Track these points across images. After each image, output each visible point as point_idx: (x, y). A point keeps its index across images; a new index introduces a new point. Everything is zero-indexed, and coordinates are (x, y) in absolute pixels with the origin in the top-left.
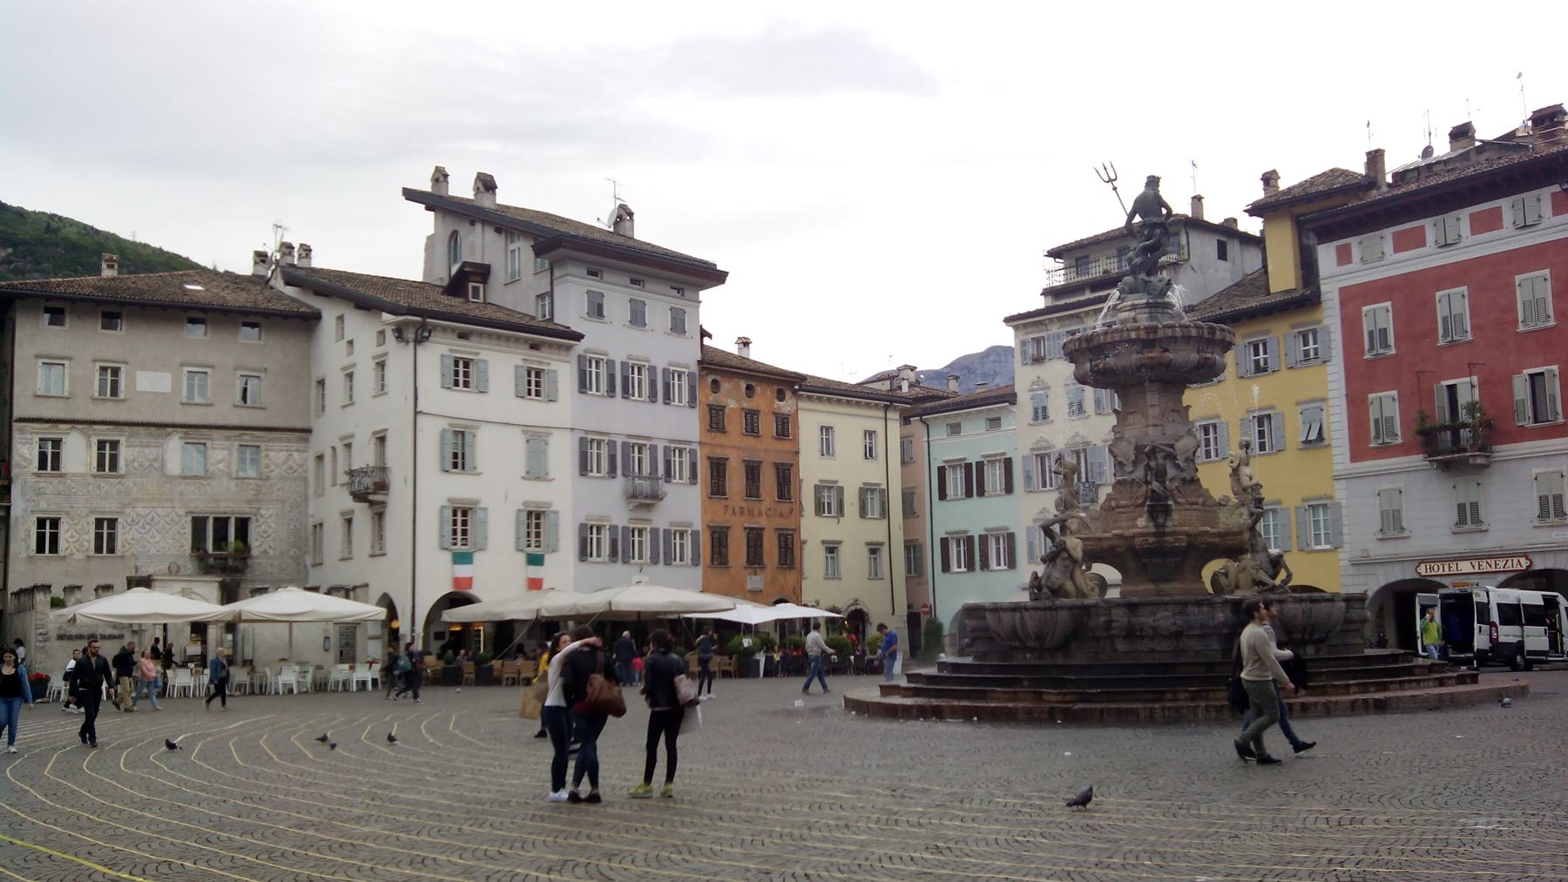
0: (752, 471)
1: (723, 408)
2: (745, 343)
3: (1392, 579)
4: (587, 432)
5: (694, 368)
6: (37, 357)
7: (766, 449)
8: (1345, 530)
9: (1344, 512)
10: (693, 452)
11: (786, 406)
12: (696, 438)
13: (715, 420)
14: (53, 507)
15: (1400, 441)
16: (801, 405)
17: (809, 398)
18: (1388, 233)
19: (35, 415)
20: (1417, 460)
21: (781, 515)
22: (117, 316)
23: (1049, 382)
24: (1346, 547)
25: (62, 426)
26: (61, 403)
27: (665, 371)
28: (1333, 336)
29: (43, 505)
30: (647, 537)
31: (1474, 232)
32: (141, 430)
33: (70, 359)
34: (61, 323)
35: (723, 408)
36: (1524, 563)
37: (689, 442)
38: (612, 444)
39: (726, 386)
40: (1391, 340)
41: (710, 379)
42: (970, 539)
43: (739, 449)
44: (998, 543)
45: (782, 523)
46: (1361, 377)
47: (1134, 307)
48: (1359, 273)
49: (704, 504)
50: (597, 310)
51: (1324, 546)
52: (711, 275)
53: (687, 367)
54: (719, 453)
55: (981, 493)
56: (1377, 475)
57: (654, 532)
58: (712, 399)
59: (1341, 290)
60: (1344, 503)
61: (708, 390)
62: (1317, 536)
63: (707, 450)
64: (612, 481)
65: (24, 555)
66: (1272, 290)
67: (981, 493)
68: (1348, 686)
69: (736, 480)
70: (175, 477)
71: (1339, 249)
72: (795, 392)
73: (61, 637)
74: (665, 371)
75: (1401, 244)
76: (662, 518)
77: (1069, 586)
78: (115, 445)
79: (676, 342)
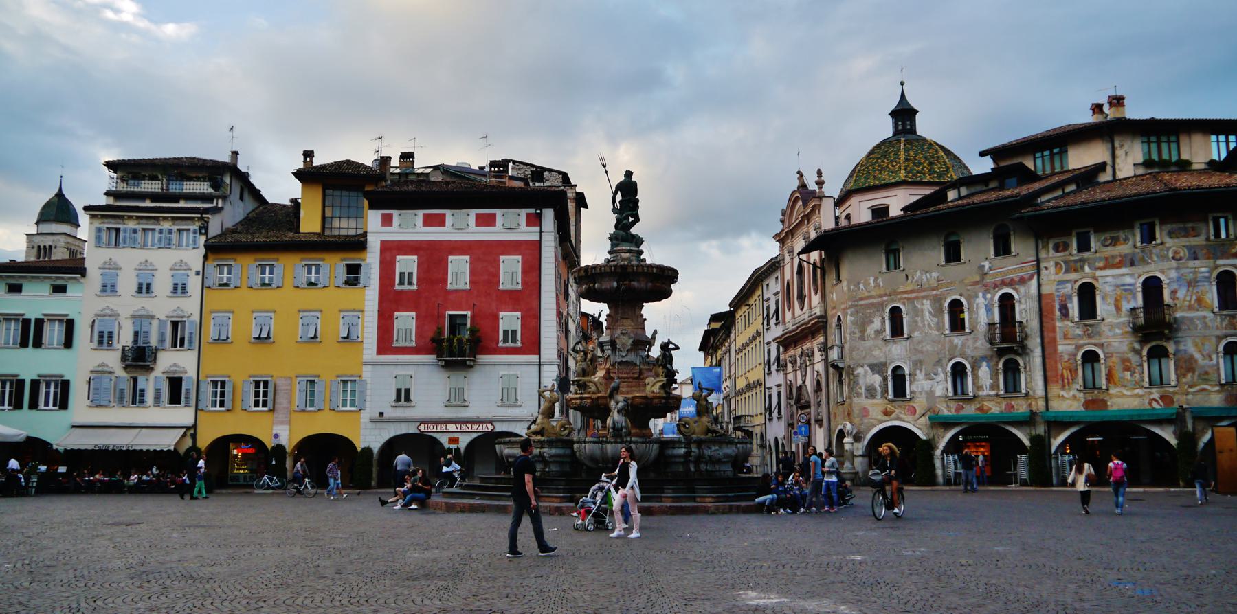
3: (399, 433)
8: (368, 399)
9: (369, 386)
15: (414, 344)
18: (420, 213)
20: (431, 358)
23: (121, 264)
24: (368, 410)
28: (373, 271)
31: (478, 224)
36: (490, 427)
40: (415, 281)
42: (23, 381)
44: (48, 387)
46: (390, 302)
47: (630, 251)
48: (395, 233)
51: (348, 408)
55: (38, 344)
56: (396, 364)
59: (383, 243)
60: (369, 381)
62: (344, 401)
66: (302, 229)
67: (38, 344)
71: (383, 215)
75: (428, 221)
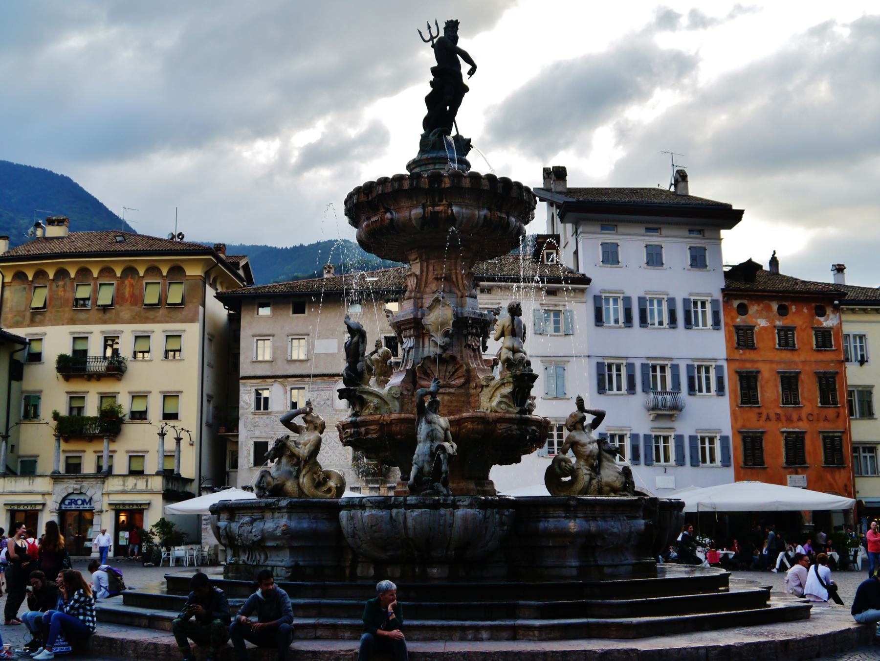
0: (790, 383)
1: (752, 328)
2: (840, 269)
4: (604, 357)
5: (718, 296)
6: (254, 336)
7: (805, 360)
10: (719, 369)
11: (829, 321)
12: (724, 355)
13: (743, 339)
14: (264, 434)
16: (844, 317)
17: (865, 311)
19: (252, 374)
21: (826, 419)
25: (268, 380)
26: (267, 366)
27: (686, 301)
29: (257, 433)
30: (672, 444)
32: (318, 380)
33: (273, 336)
35: (752, 328)
37: (715, 360)
38: (630, 367)
39: (753, 309)
41: (736, 303)
43: (772, 362)
45: (827, 427)
49: (733, 413)
50: (610, 256)
52: (729, 216)
53: (710, 295)
54: (749, 367)
57: (679, 439)
58: (739, 320)
61: (734, 313)
63: (736, 366)
64: (632, 398)
65: (246, 467)
68: (477, 629)
69: (770, 391)
72: (836, 309)
74: (686, 301)
76: (686, 427)
77: (290, 486)
79: (697, 275)
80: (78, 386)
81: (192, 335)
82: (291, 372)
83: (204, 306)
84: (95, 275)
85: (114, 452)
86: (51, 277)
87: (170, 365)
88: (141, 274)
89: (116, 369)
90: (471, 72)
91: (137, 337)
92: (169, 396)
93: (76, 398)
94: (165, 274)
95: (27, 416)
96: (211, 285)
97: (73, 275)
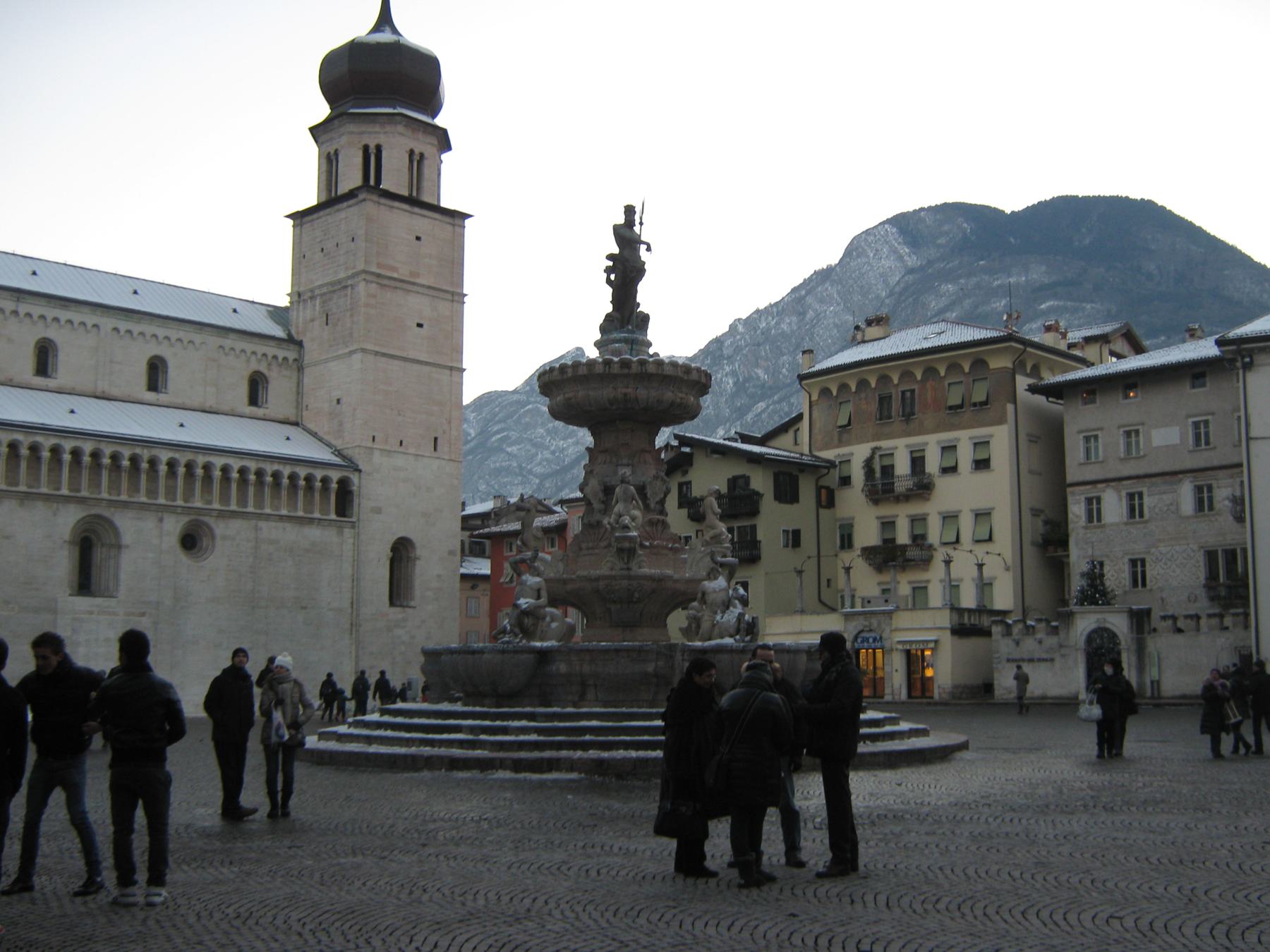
22: (1203, 375)
25: (1100, 486)
34: (1094, 401)
70: (1188, 518)
73: (1008, 660)
78: (1141, 495)
80: (887, 510)
81: (1001, 439)
82: (1126, 473)
83: (1015, 402)
84: (896, 382)
85: (928, 581)
86: (853, 389)
87: (982, 476)
88: (942, 374)
89: (923, 488)
90: (649, 249)
91: (943, 448)
92: (982, 515)
93: (888, 525)
94: (967, 370)
95: (842, 547)
96: (1028, 375)
97: (873, 385)
